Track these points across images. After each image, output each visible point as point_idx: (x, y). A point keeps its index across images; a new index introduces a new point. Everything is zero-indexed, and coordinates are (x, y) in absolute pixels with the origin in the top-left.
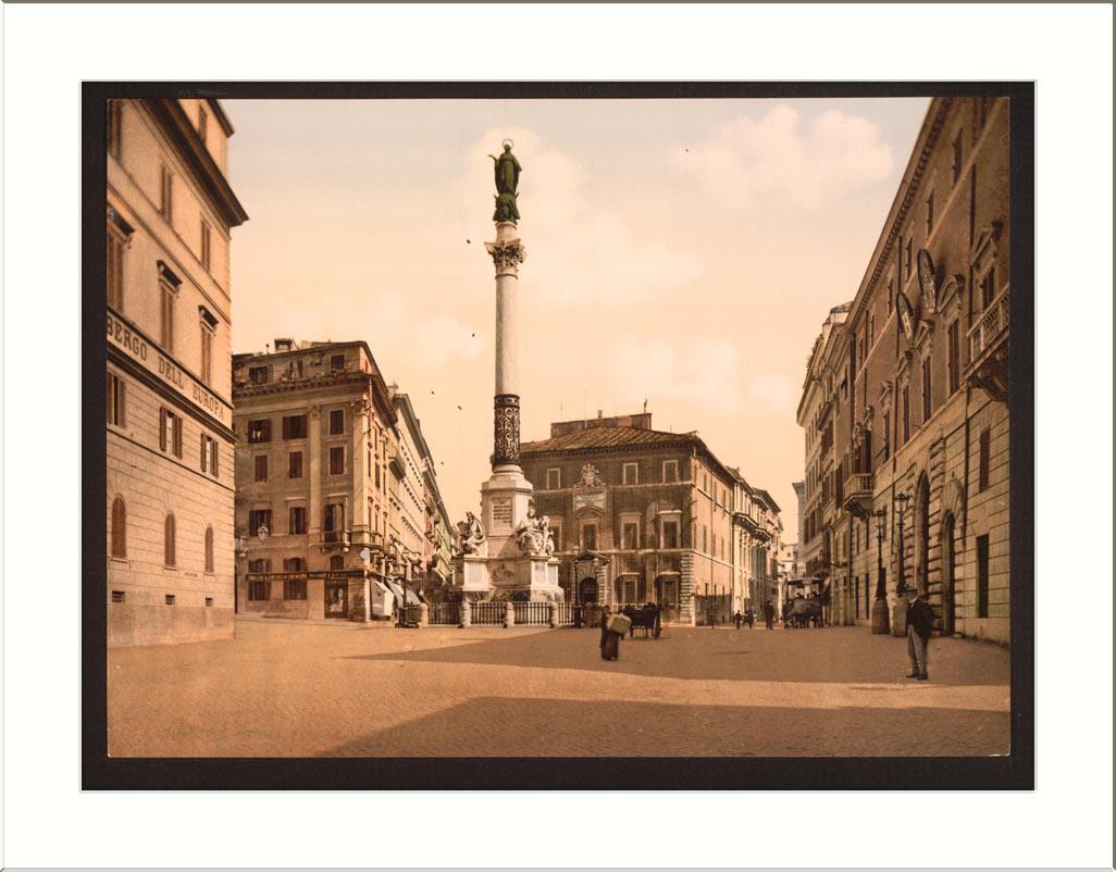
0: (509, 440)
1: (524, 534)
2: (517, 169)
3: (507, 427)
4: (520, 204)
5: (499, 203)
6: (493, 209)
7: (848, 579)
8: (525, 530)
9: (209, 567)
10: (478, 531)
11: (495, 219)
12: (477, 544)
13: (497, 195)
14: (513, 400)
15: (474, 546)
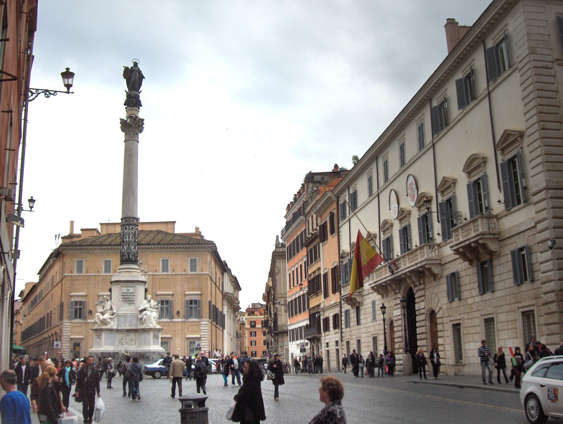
0: (132, 247)
1: (145, 312)
2: (142, 77)
3: (131, 239)
4: (143, 97)
5: (129, 96)
6: (125, 98)
7: (339, 342)
8: (145, 310)
9: (457, 327)
10: (111, 309)
11: (125, 105)
12: (111, 319)
13: (127, 91)
14: (135, 221)
15: (109, 321)
